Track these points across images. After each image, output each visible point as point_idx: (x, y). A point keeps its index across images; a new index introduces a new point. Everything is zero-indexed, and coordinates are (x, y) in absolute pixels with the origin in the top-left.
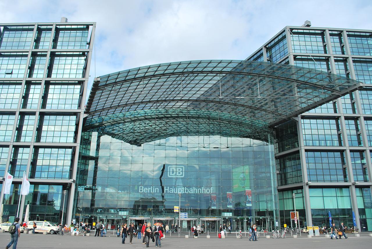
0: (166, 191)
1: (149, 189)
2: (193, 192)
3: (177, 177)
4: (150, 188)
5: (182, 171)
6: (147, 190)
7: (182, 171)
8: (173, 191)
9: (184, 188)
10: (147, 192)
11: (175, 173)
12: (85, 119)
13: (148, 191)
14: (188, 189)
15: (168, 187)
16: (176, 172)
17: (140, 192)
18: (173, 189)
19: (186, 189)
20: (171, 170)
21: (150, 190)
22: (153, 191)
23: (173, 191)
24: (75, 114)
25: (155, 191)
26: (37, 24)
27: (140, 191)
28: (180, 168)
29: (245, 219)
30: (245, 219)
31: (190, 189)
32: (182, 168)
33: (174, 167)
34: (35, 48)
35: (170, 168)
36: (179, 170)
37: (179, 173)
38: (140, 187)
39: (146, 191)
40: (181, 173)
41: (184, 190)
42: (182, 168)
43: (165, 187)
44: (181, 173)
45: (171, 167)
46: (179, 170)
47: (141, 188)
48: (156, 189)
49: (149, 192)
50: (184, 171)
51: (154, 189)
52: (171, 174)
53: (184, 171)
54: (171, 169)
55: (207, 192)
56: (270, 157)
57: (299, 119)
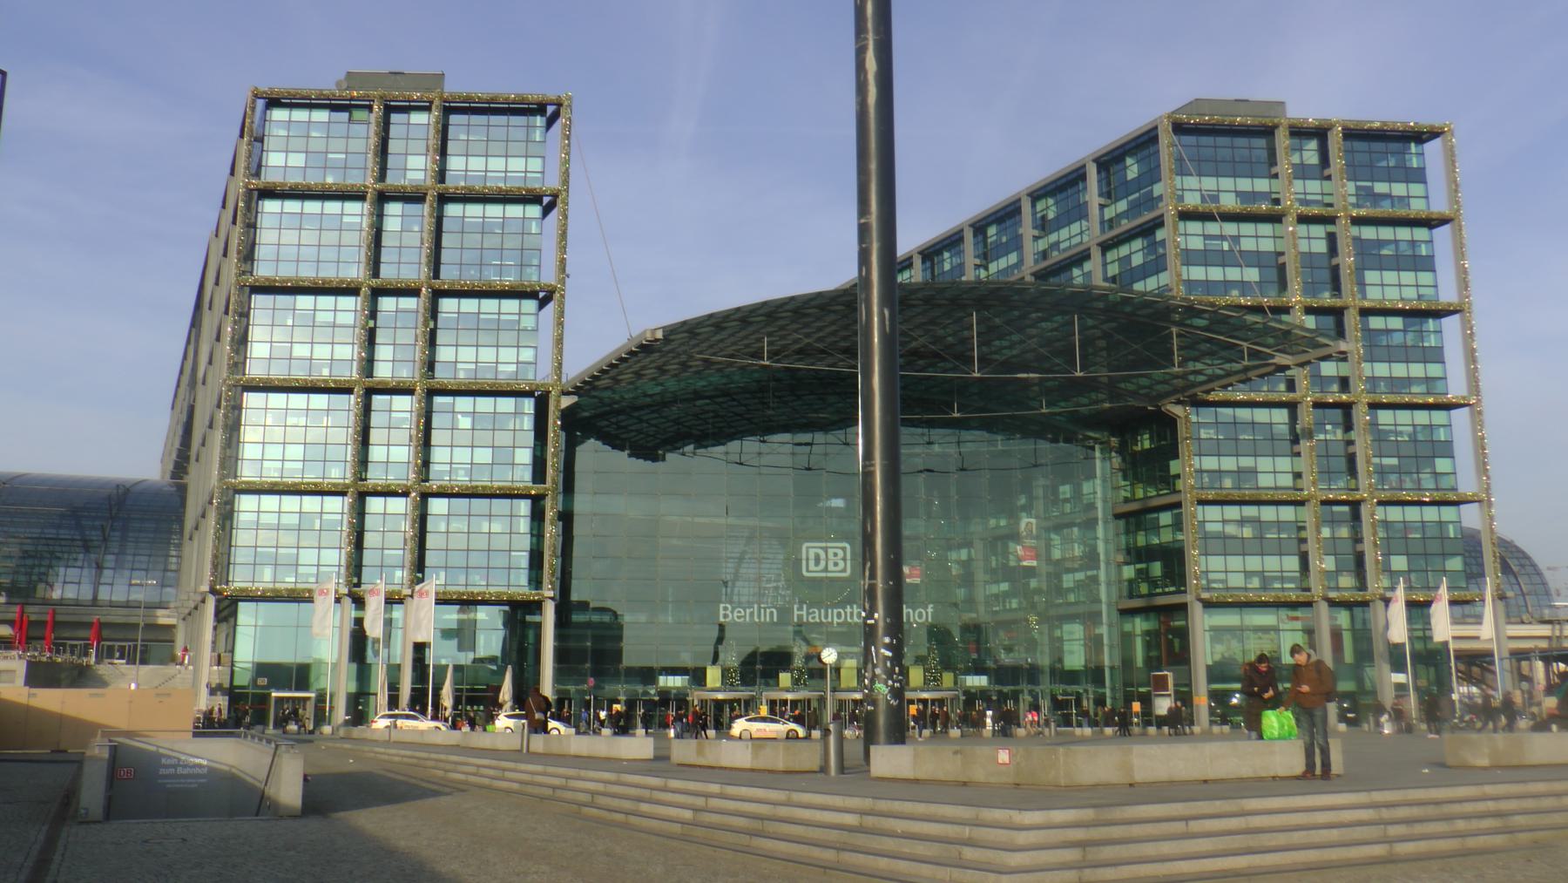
0: (800, 617)
3: (829, 575)
6: (743, 613)
7: (844, 559)
9: (852, 608)
13: (745, 616)
15: (805, 606)
16: (827, 559)
19: (856, 611)
20: (812, 556)
21: (752, 614)
28: (836, 550)
29: (1026, 692)
30: (1026, 692)
33: (821, 548)
35: (808, 548)
36: (835, 555)
37: (836, 564)
39: (739, 617)
40: (841, 564)
41: (852, 614)
42: (844, 549)
44: (841, 564)
46: (835, 555)
49: (748, 619)
51: (762, 611)
55: (917, 618)
56: (1100, 515)
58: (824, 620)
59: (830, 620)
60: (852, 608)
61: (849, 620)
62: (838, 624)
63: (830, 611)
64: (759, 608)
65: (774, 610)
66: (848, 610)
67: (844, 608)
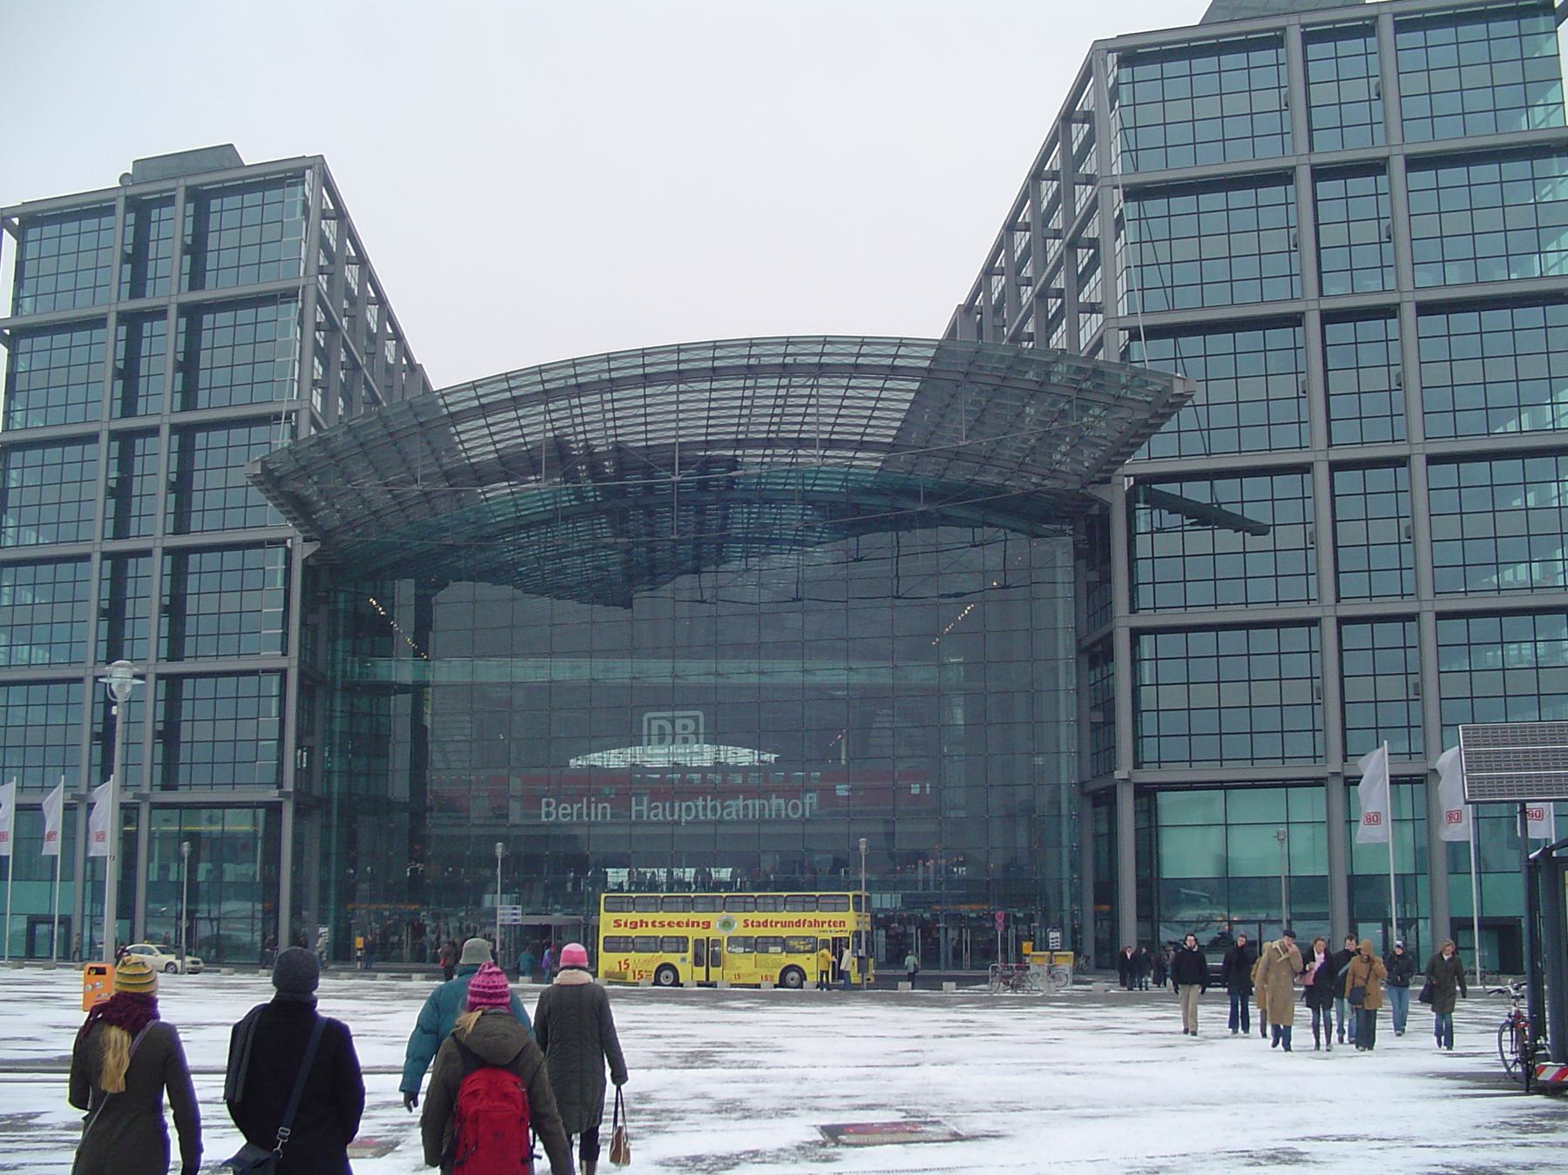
4: (580, 805)
6: (569, 811)
7: (696, 733)
8: (664, 815)
9: (705, 800)
12: (305, 561)
13: (571, 814)
14: (718, 805)
16: (674, 735)
19: (710, 804)
20: (655, 731)
22: (589, 815)
23: (664, 815)
25: (596, 816)
27: (543, 816)
30: (942, 918)
31: (726, 804)
32: (696, 719)
34: (132, 296)
36: (685, 727)
38: (544, 800)
39: (564, 815)
41: (705, 808)
42: (696, 719)
43: (633, 799)
45: (655, 718)
46: (685, 727)
47: (548, 805)
48: (600, 806)
49: (575, 819)
50: (702, 731)
51: (593, 805)
53: (702, 731)
54: (655, 724)
57: (1115, 495)
59: (676, 817)
60: (705, 800)
62: (687, 822)
63: (677, 804)
64: (589, 802)
65: (606, 804)
66: (700, 803)
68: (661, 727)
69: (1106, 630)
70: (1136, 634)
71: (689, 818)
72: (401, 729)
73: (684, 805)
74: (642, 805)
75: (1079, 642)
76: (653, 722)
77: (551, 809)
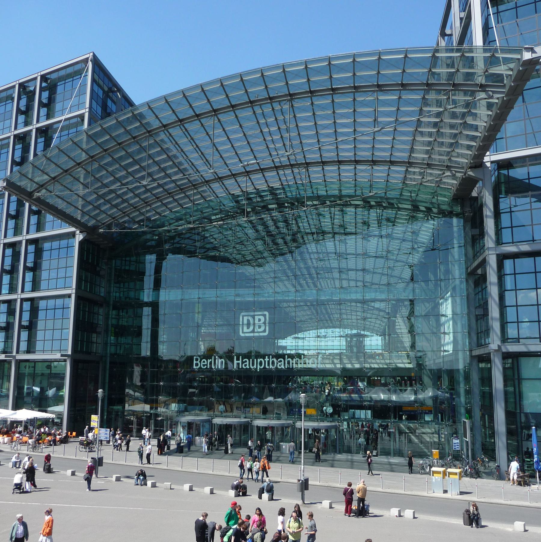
0: (238, 364)
1: (209, 361)
2: (285, 365)
5: (265, 323)
6: (206, 363)
8: (249, 365)
9: (269, 358)
10: (206, 367)
11: (251, 328)
12: (81, 243)
13: (207, 365)
15: (241, 357)
17: (195, 367)
18: (249, 361)
20: (245, 322)
21: (211, 363)
23: (249, 365)
24: (73, 235)
26: (17, 82)
36: (259, 320)
39: (204, 365)
41: (269, 362)
42: (264, 316)
43: (235, 357)
46: (259, 320)
47: (197, 360)
52: (245, 330)
54: (246, 318)
58: (252, 367)
59: (255, 367)
61: (267, 367)
63: (255, 360)
66: (267, 359)
67: (264, 358)
68: (248, 320)
69: (480, 259)
70: (502, 258)
71: (262, 367)
72: (146, 323)
73: (259, 360)
74: (239, 360)
75: (467, 269)
76: (245, 317)
77: (198, 362)
